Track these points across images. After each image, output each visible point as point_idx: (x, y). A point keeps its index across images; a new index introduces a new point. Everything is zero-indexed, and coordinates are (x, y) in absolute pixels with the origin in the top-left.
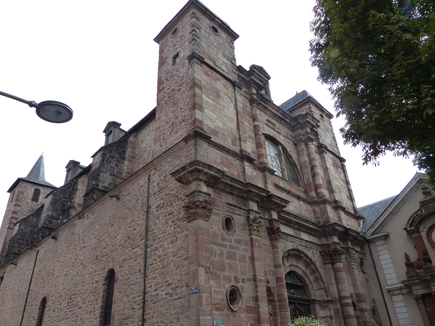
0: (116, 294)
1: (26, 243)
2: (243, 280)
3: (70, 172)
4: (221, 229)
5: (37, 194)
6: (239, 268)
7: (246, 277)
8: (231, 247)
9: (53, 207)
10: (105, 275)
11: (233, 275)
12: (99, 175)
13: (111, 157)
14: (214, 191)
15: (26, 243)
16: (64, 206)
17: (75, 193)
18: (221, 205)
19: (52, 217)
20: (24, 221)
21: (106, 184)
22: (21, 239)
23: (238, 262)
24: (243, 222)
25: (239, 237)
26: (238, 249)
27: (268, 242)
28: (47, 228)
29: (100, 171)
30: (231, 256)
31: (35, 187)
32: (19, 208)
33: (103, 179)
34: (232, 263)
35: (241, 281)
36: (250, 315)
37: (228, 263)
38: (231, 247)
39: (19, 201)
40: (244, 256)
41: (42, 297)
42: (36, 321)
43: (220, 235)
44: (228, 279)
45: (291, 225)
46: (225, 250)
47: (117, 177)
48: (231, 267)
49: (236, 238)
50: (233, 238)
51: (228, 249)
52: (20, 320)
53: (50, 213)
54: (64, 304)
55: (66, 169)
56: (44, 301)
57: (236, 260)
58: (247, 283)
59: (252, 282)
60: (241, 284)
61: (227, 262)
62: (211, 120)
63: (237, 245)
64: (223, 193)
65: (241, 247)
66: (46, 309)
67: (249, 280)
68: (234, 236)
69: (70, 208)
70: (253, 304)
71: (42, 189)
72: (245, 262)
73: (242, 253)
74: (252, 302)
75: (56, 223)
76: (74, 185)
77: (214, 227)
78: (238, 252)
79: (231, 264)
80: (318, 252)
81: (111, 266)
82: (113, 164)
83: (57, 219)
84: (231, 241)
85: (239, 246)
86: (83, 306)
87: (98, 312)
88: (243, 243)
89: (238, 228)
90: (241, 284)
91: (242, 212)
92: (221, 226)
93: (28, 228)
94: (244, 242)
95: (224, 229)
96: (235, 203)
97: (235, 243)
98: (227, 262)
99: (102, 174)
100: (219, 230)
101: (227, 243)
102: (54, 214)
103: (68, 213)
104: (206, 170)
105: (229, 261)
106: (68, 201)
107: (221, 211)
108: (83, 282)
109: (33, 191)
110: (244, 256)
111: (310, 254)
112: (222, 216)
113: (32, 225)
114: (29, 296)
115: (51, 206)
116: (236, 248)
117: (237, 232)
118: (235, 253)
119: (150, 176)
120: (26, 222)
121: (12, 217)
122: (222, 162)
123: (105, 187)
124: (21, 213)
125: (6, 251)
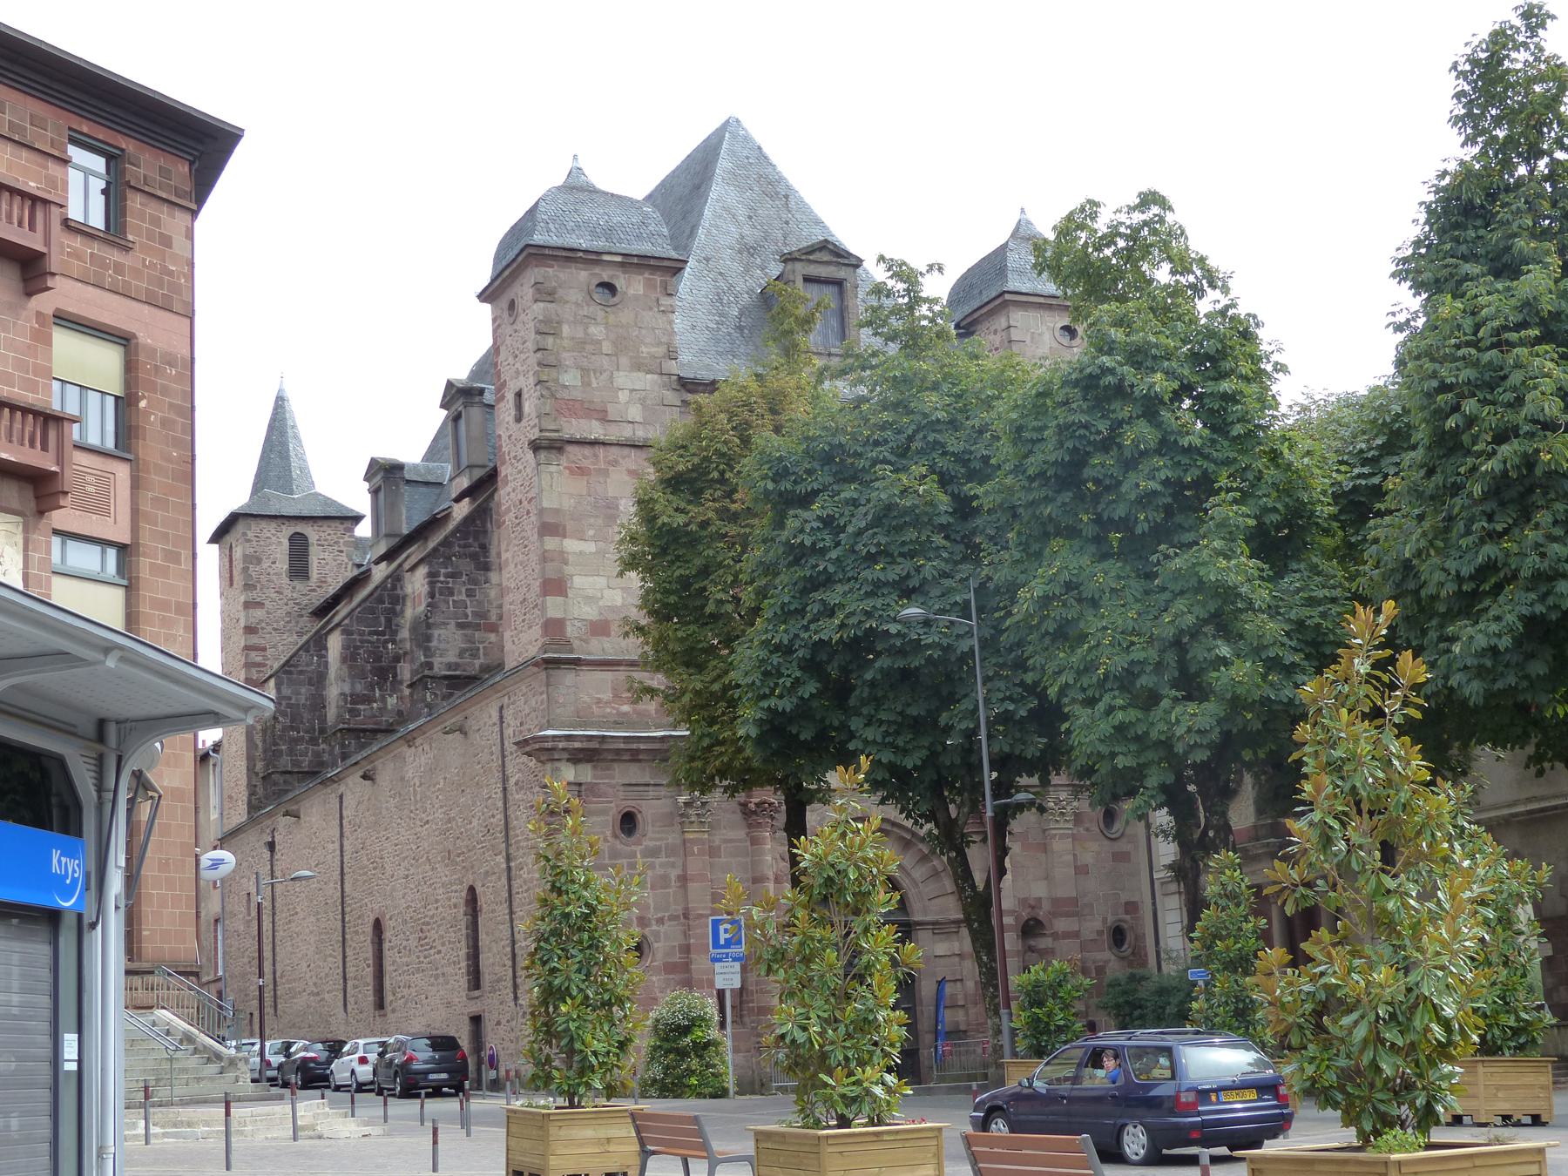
0: (482, 936)
1: (307, 736)
2: (660, 921)
3: (381, 495)
5: (299, 550)
9: (350, 668)
10: (464, 894)
12: (428, 638)
13: (453, 575)
14: (595, 767)
15: (307, 736)
16: (378, 659)
17: (402, 611)
18: (610, 790)
19: (356, 699)
20: (287, 672)
21: (452, 657)
22: (292, 728)
24: (667, 810)
25: (652, 844)
27: (741, 833)
28: (349, 730)
29: (429, 626)
31: (289, 530)
32: (259, 613)
33: (442, 646)
39: (255, 587)
41: (372, 919)
42: (371, 969)
47: (477, 627)
52: (340, 957)
53: (347, 689)
54: (413, 943)
55: (367, 485)
56: (378, 926)
60: (654, 927)
62: (590, 599)
64: (615, 765)
65: (657, 861)
66: (386, 945)
67: (673, 918)
69: (397, 659)
71: (312, 533)
75: (368, 713)
76: (394, 588)
81: (469, 879)
82: (460, 593)
83: (368, 700)
86: (443, 949)
87: (464, 964)
90: (654, 927)
91: (663, 792)
92: (609, 833)
93: (303, 690)
95: (615, 836)
96: (647, 779)
99: (436, 633)
100: (605, 840)
102: (359, 688)
103: (395, 676)
104: (561, 745)
106: (386, 642)
108: (437, 901)
109: (286, 543)
113: (310, 679)
114: (347, 909)
115: (345, 668)
117: (650, 834)
119: (502, 708)
120: (290, 673)
121: (247, 648)
122: (615, 696)
123: (449, 666)
124: (269, 629)
125: (259, 753)
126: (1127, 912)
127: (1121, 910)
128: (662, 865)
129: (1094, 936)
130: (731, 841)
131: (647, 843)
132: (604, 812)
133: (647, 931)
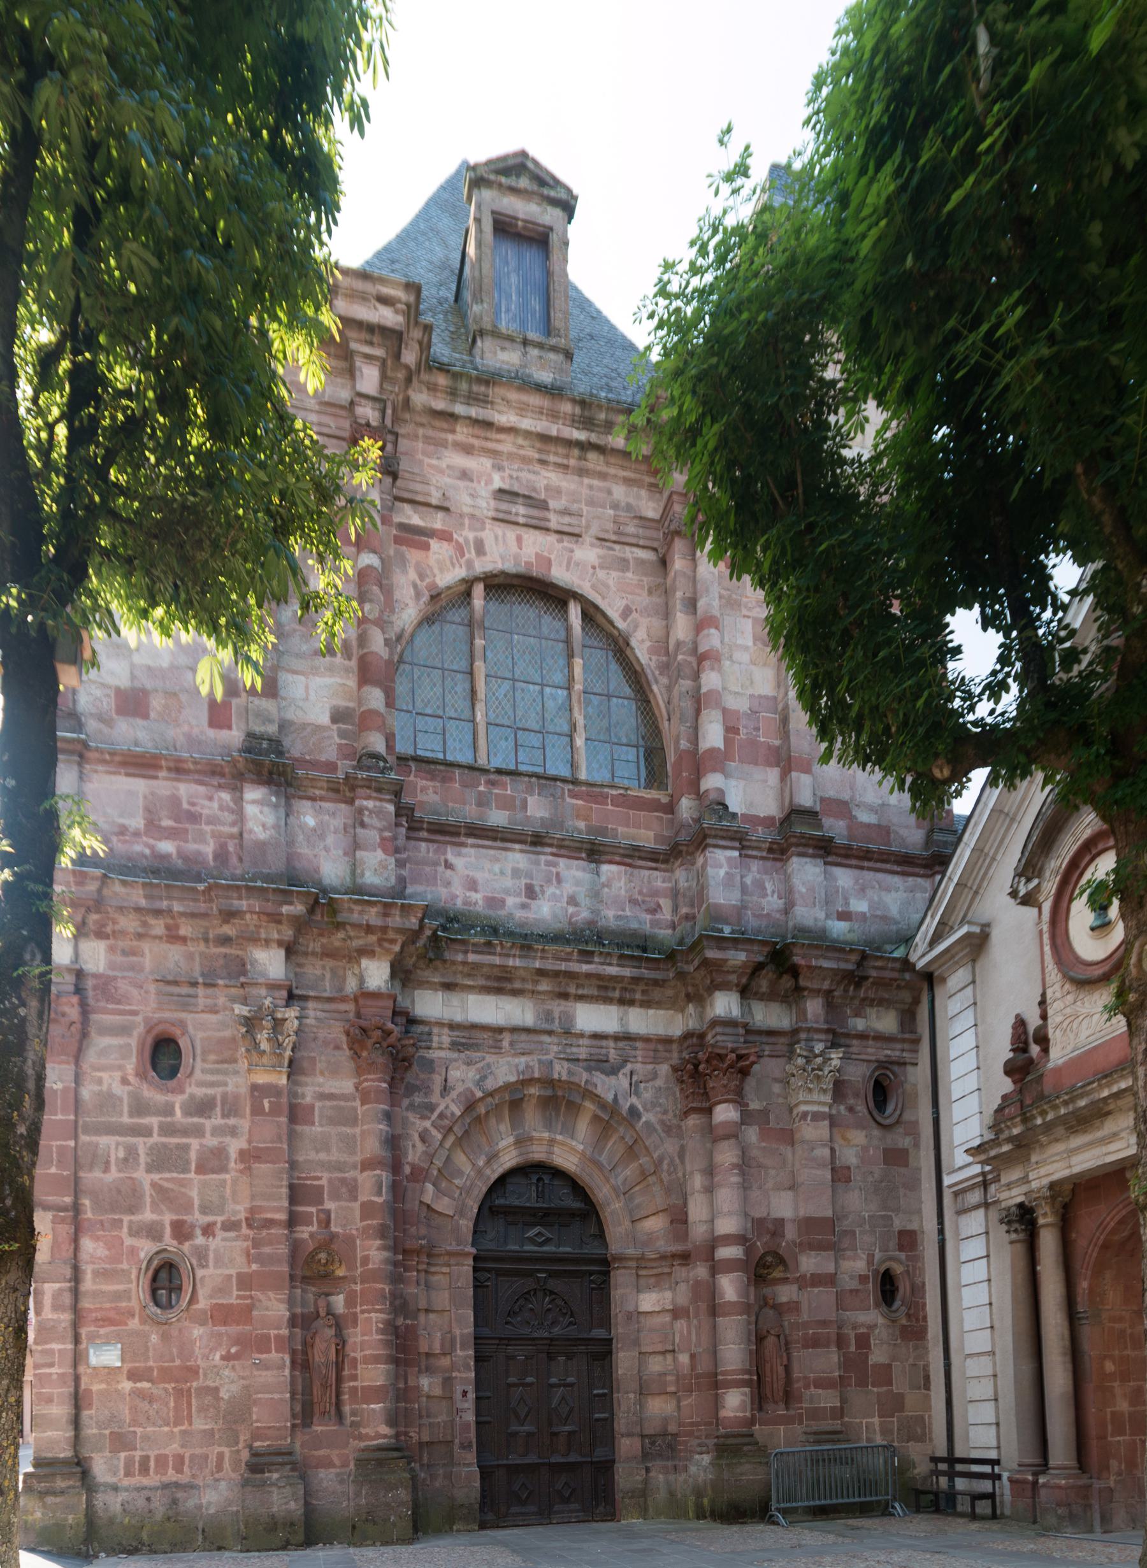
2: (208, 1230)
4: (131, 1079)
6: (194, 1194)
7: (219, 1219)
8: (168, 1130)
11: (168, 1218)
18: (135, 992)
23: (192, 1175)
25: (200, 1092)
26: (198, 1132)
30: (162, 1160)
34: (167, 1180)
35: (198, 1232)
36: (223, 1329)
37: (154, 1185)
38: (168, 1130)
40: (220, 1153)
43: (125, 1097)
44: (152, 1232)
45: (517, 985)
46: (142, 1145)
48: (163, 1194)
49: (192, 1097)
50: (178, 1100)
51: (156, 1138)
57: (186, 1170)
58: (220, 1234)
59: (245, 1230)
61: (145, 1178)
63: (196, 1120)
65: (208, 1124)
68: (182, 1092)
70: (238, 1297)
72: (223, 1169)
73: (211, 1141)
74: (235, 1293)
77: (104, 1075)
78: (195, 1143)
79: (166, 1184)
80: (664, 1069)
84: (168, 1110)
85: (202, 1120)
88: (218, 1109)
89: (204, 1061)
90: (200, 1240)
92: (130, 1066)
94: (223, 1105)
95: (141, 1075)
97: (187, 1113)
98: (145, 1178)
100: (125, 1081)
101: (154, 1121)
105: (156, 1177)
107: (135, 1013)
110: (220, 1153)
111: (608, 1086)
112: (140, 1029)
116: (185, 1132)
117: (198, 1074)
118: (186, 1148)
126: (901, 1248)
127: (893, 1243)
128: (217, 1131)
129: (854, 1284)
130: (331, 1097)
131: (194, 1090)
132: (124, 1030)
133: (186, 1247)
